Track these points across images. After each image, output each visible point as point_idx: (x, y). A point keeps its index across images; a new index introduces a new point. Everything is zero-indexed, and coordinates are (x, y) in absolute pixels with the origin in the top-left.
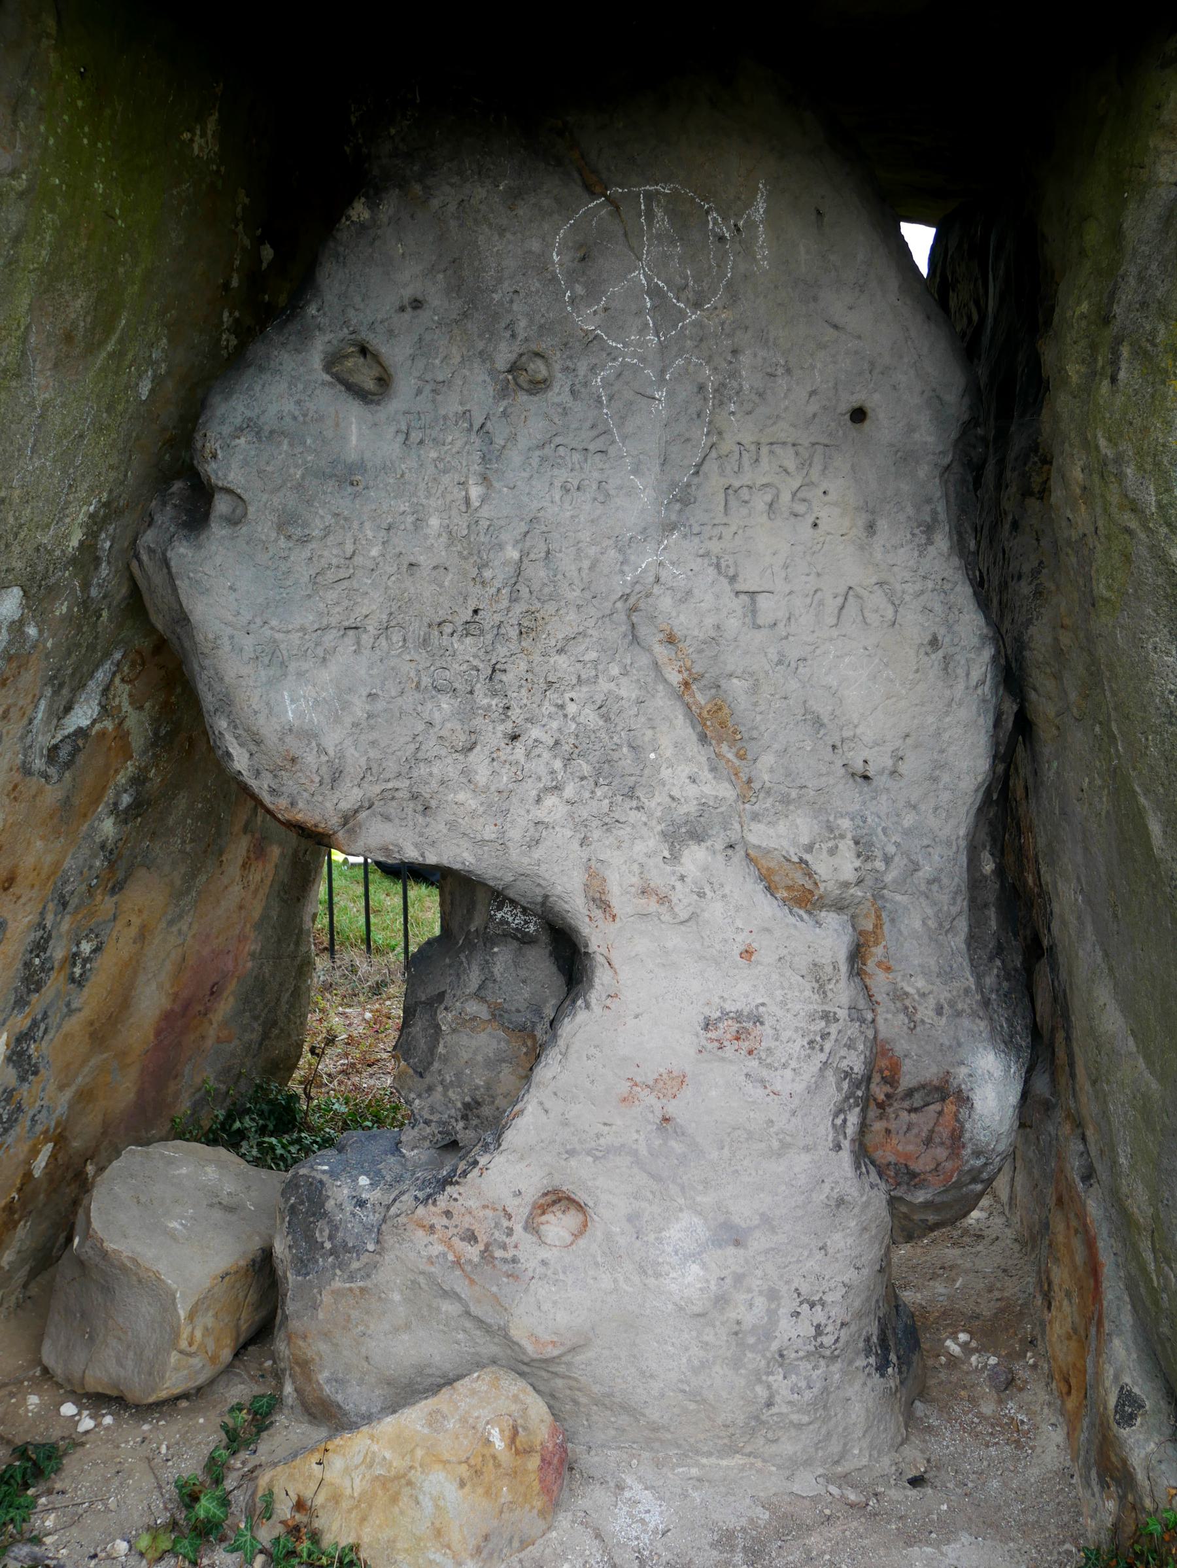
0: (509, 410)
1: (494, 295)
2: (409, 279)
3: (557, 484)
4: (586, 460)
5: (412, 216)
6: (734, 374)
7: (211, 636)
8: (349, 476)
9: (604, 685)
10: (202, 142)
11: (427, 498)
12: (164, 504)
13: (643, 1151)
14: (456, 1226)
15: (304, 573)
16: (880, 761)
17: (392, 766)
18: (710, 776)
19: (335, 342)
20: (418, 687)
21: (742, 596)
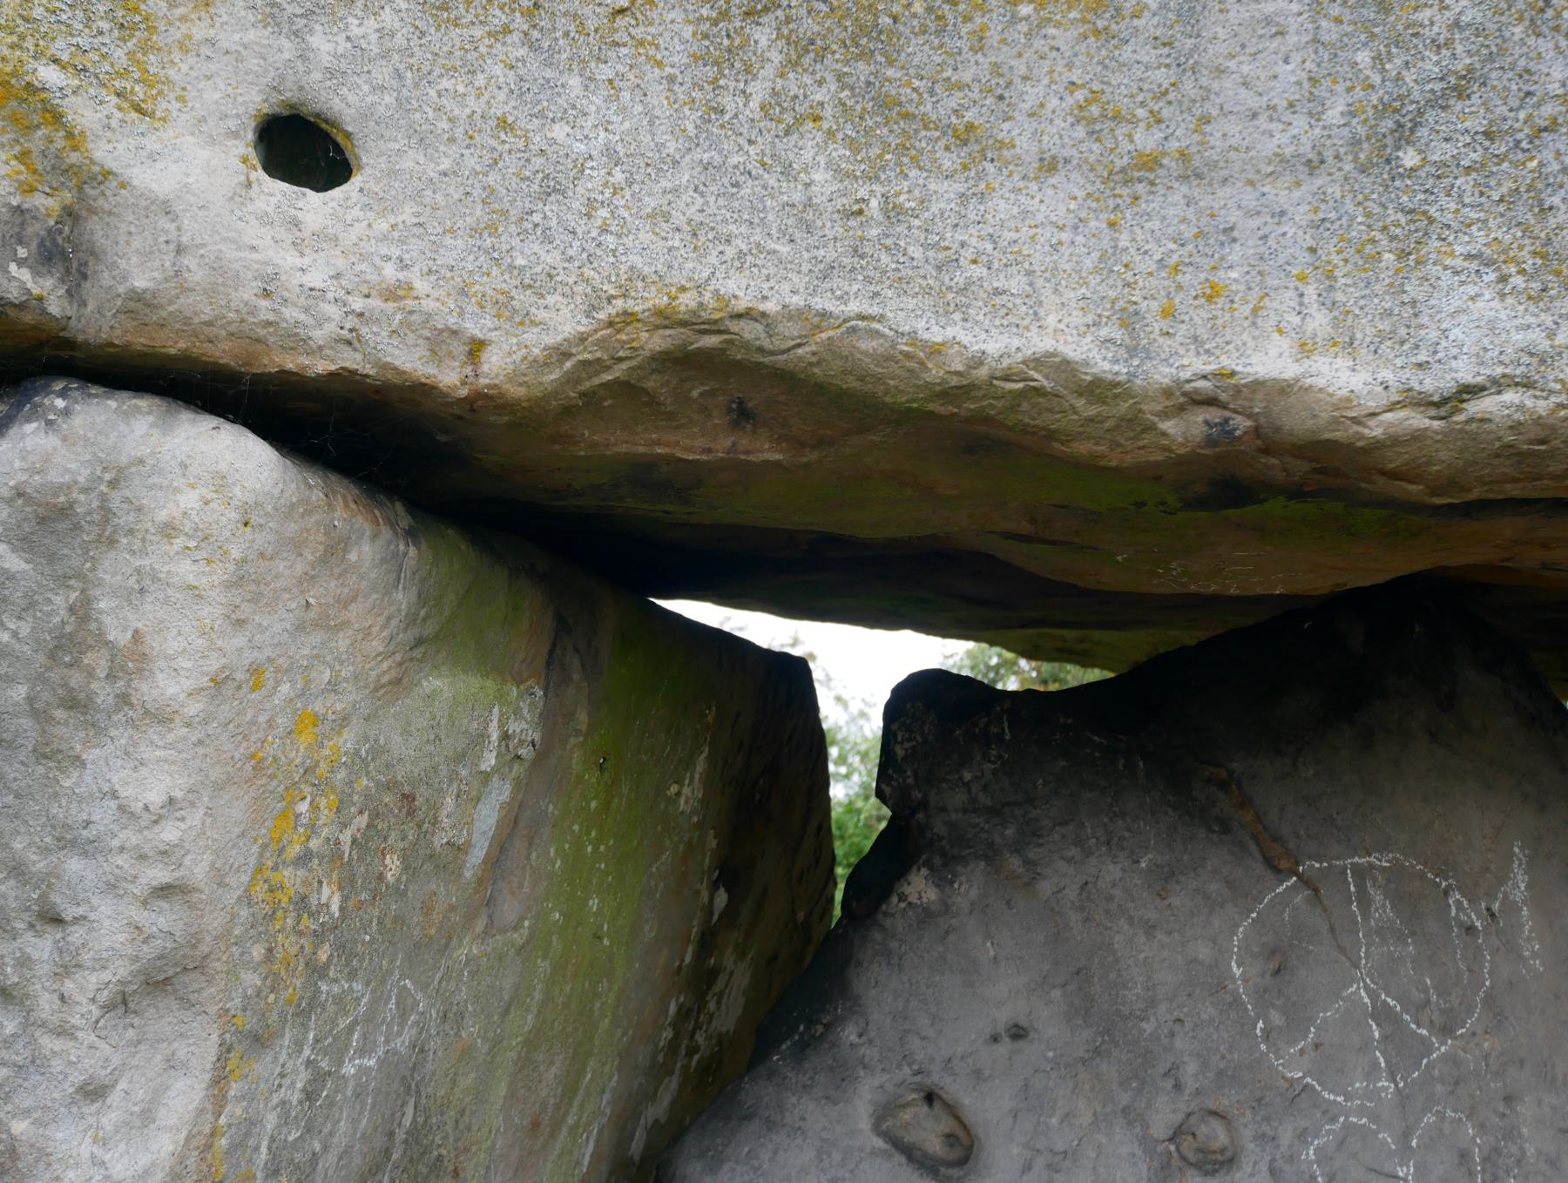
1: (1144, 1025)
2: (1007, 993)
6: (1511, 1134)
10: (688, 794)
19: (889, 1087)
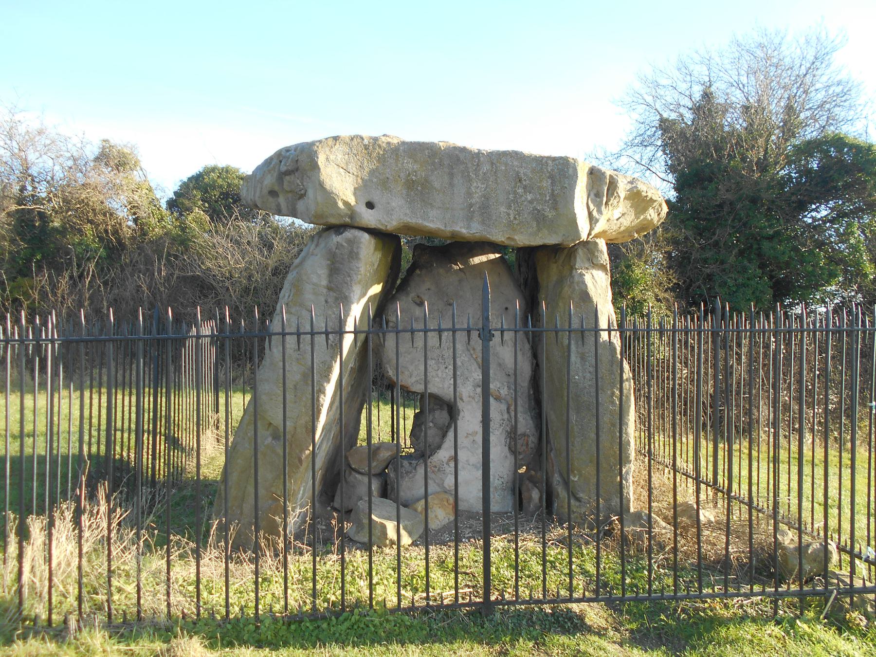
2: (428, 284)
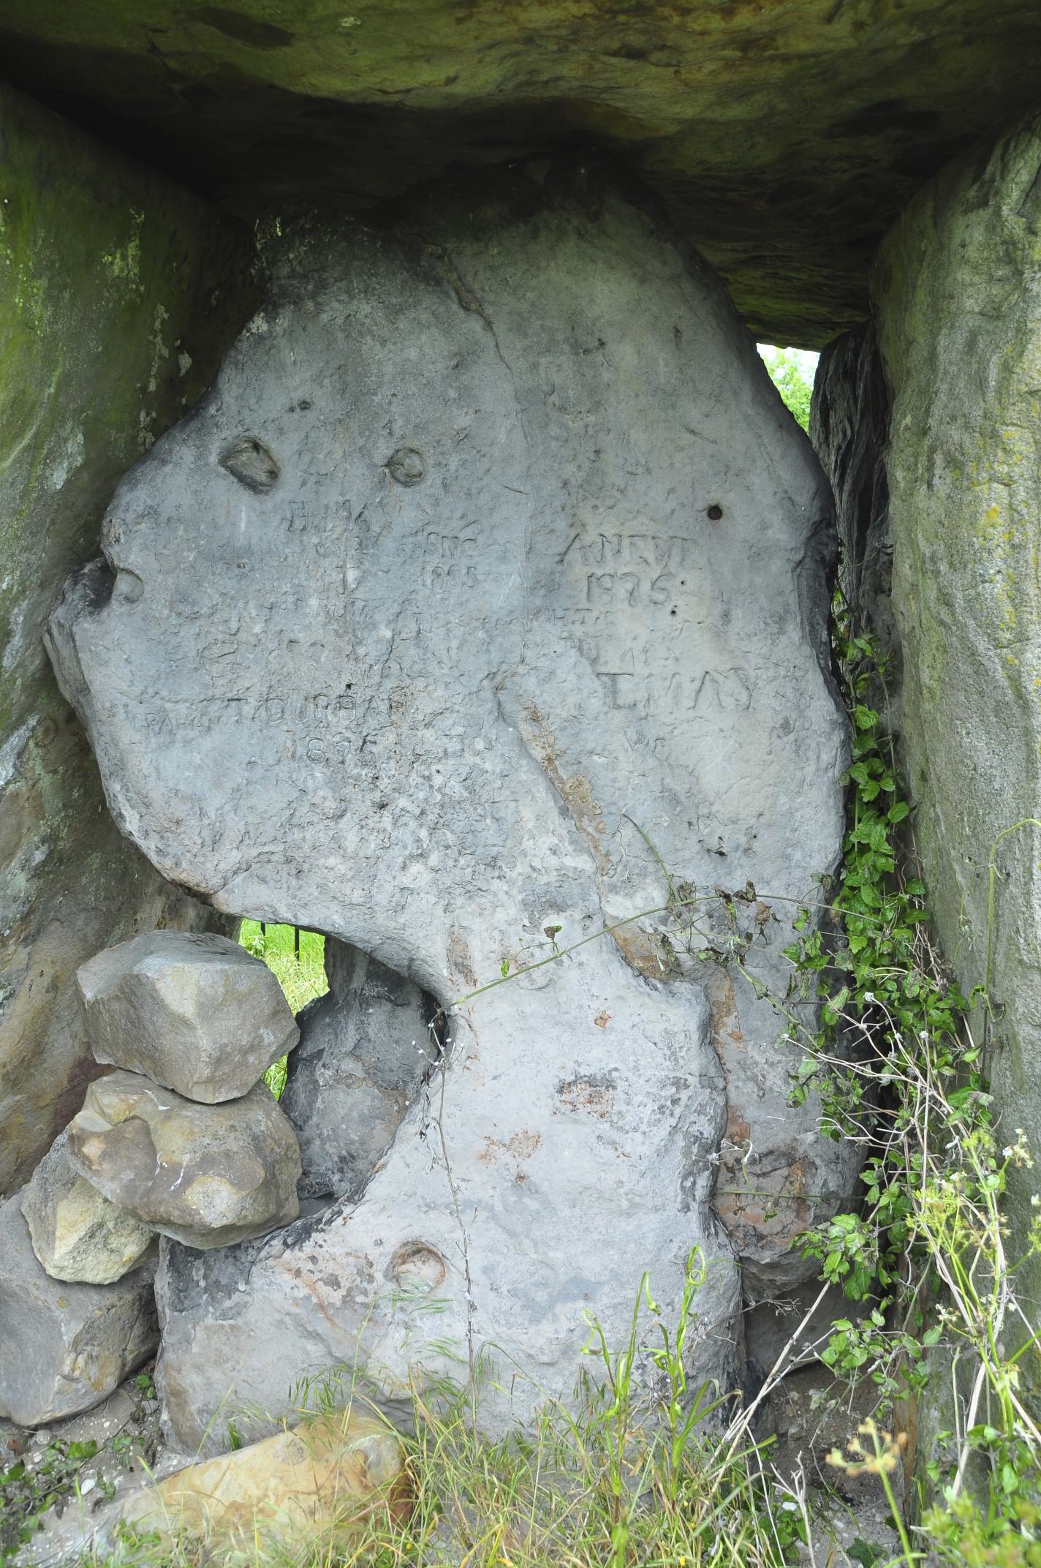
0: (385, 501)
2: (298, 383)
3: (429, 569)
4: (456, 548)
5: (304, 329)
7: (108, 705)
8: (235, 560)
9: (470, 759)
11: (307, 580)
12: (76, 583)
13: (499, 1207)
14: (321, 1271)
15: (191, 647)
16: (734, 839)
17: (269, 830)
18: (570, 848)
19: (230, 439)
20: (293, 756)
21: (604, 678)
